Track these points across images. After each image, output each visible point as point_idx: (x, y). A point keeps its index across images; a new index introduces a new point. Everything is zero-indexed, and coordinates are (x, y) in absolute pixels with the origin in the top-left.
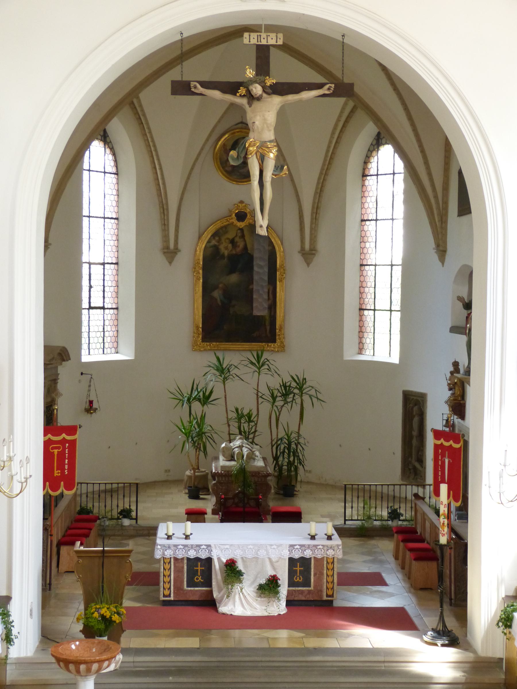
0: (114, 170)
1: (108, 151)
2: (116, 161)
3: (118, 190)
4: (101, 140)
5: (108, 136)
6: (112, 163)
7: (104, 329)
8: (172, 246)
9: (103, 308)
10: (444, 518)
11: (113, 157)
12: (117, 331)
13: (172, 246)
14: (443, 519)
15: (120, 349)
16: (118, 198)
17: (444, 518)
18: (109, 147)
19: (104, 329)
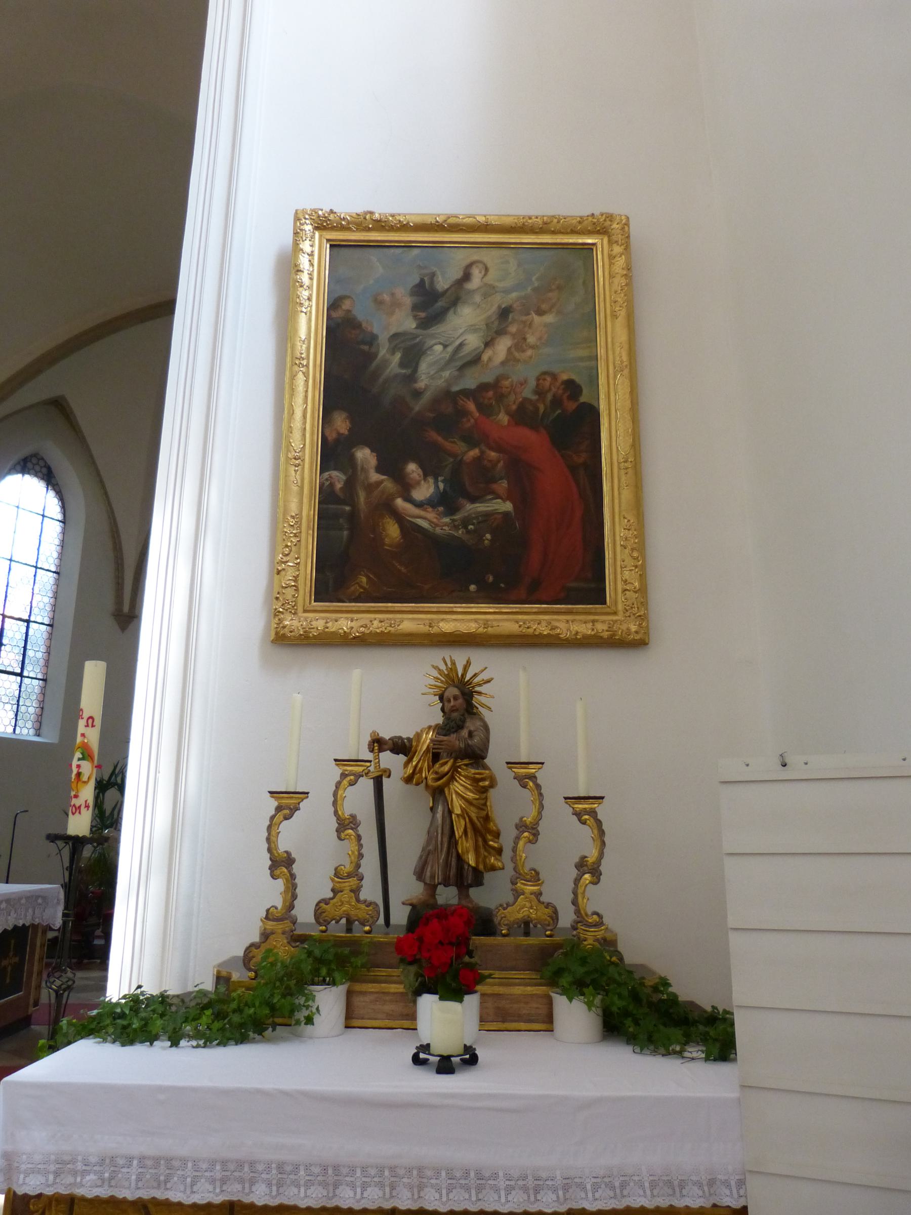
0: (60, 517)
1: (51, 494)
2: (63, 507)
3: (63, 541)
4: (42, 479)
5: (55, 477)
6: (58, 509)
7: (18, 701)
8: (126, 609)
9: (21, 675)
10: (81, 756)
11: (60, 502)
12: (42, 708)
13: (126, 609)
14: (79, 759)
15: (44, 730)
16: (62, 549)
17: (81, 756)
18: (54, 490)
19: (18, 701)
